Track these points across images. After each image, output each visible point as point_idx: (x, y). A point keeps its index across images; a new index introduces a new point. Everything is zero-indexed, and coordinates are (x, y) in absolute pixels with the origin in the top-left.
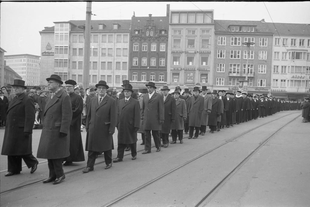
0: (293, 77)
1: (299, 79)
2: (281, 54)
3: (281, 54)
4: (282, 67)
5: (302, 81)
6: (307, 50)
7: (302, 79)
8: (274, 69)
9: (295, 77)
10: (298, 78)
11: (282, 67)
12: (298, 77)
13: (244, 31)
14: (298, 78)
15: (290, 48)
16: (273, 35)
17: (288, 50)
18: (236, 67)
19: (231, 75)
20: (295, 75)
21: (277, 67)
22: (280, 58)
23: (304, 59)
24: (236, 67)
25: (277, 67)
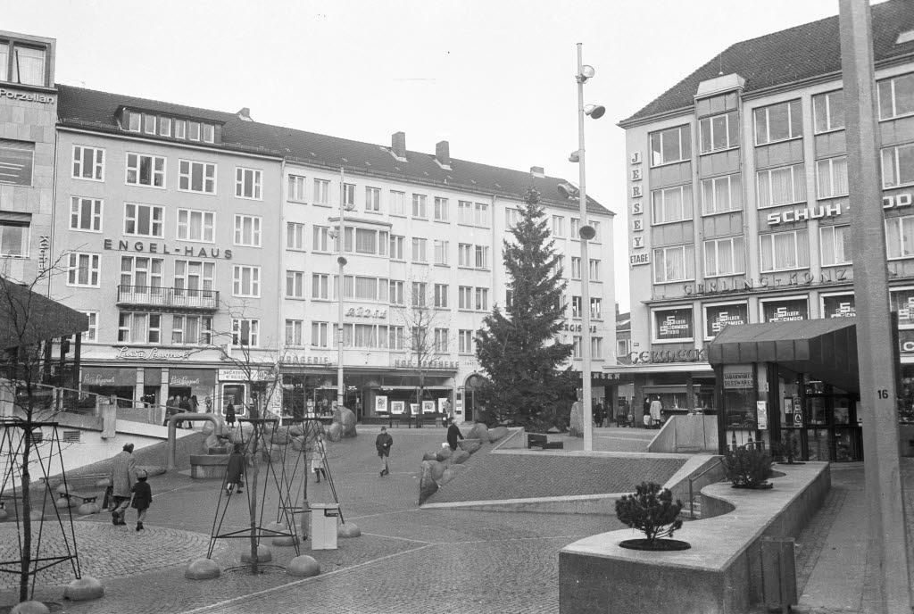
0: (350, 315)
1: (370, 321)
2: (308, 232)
3: (308, 232)
4: (315, 276)
5: (380, 326)
6: (390, 226)
7: (379, 322)
8: (290, 281)
9: (356, 313)
10: (366, 317)
11: (315, 276)
12: (365, 314)
13: (177, 137)
14: (366, 317)
15: (335, 213)
16: (284, 162)
17: (331, 220)
18: (148, 269)
19: (127, 299)
20: (356, 307)
21: (299, 274)
22: (307, 244)
23: (382, 252)
24: (148, 269)
25: (299, 274)
